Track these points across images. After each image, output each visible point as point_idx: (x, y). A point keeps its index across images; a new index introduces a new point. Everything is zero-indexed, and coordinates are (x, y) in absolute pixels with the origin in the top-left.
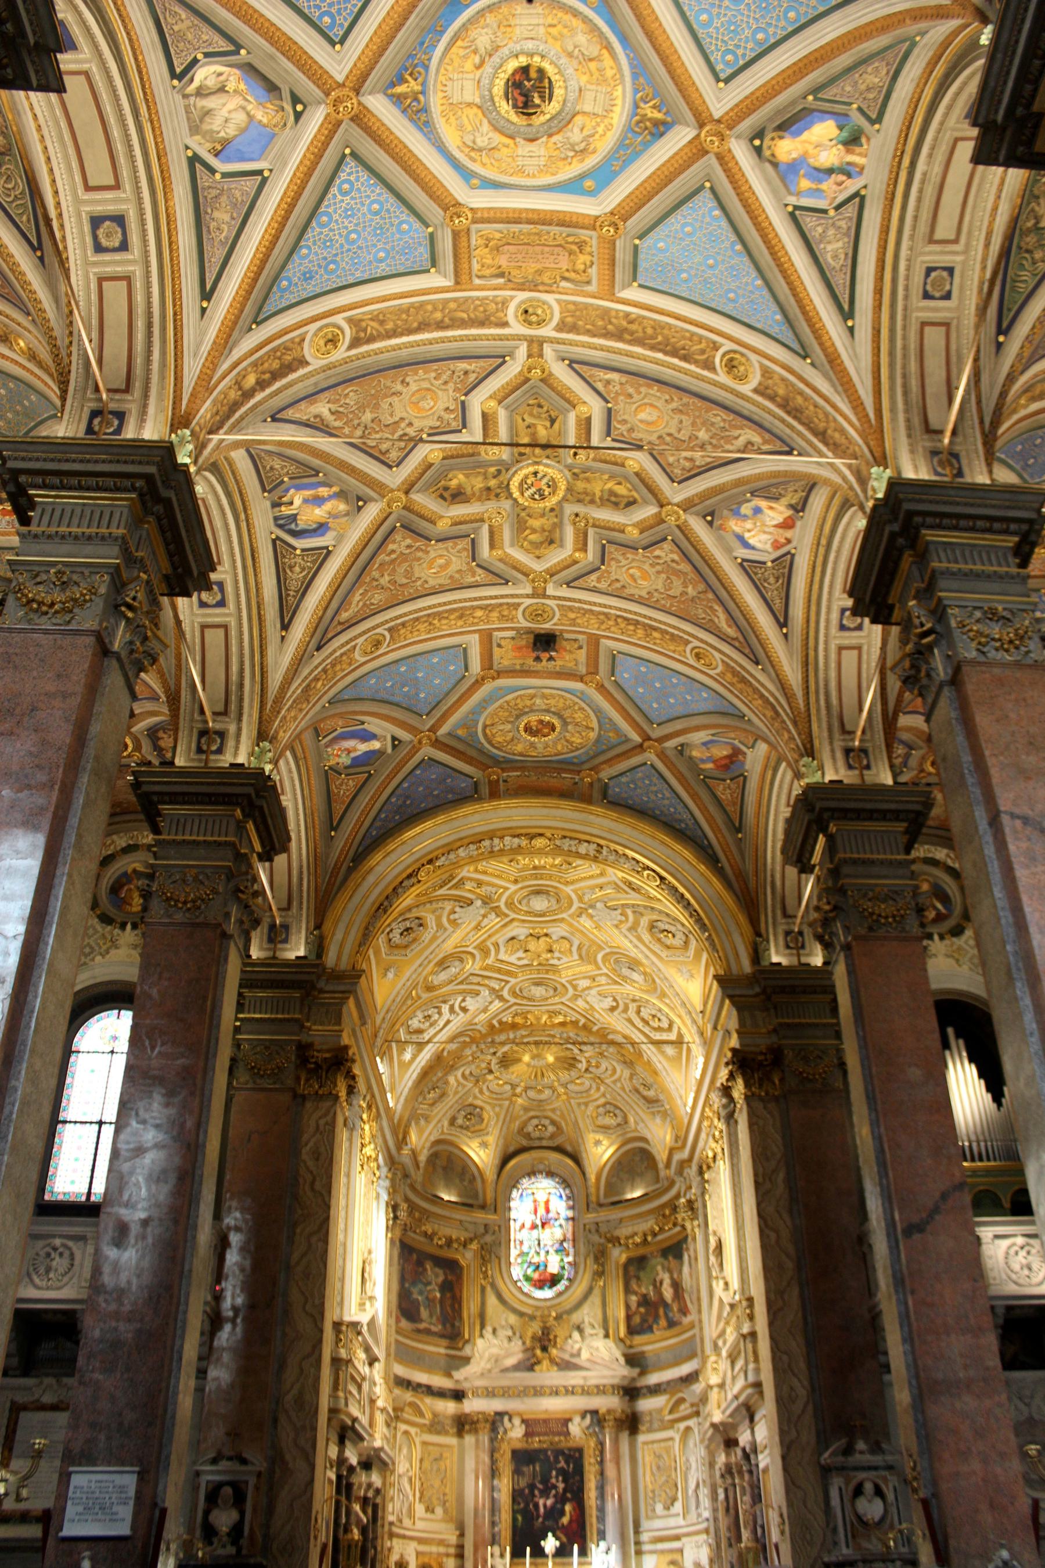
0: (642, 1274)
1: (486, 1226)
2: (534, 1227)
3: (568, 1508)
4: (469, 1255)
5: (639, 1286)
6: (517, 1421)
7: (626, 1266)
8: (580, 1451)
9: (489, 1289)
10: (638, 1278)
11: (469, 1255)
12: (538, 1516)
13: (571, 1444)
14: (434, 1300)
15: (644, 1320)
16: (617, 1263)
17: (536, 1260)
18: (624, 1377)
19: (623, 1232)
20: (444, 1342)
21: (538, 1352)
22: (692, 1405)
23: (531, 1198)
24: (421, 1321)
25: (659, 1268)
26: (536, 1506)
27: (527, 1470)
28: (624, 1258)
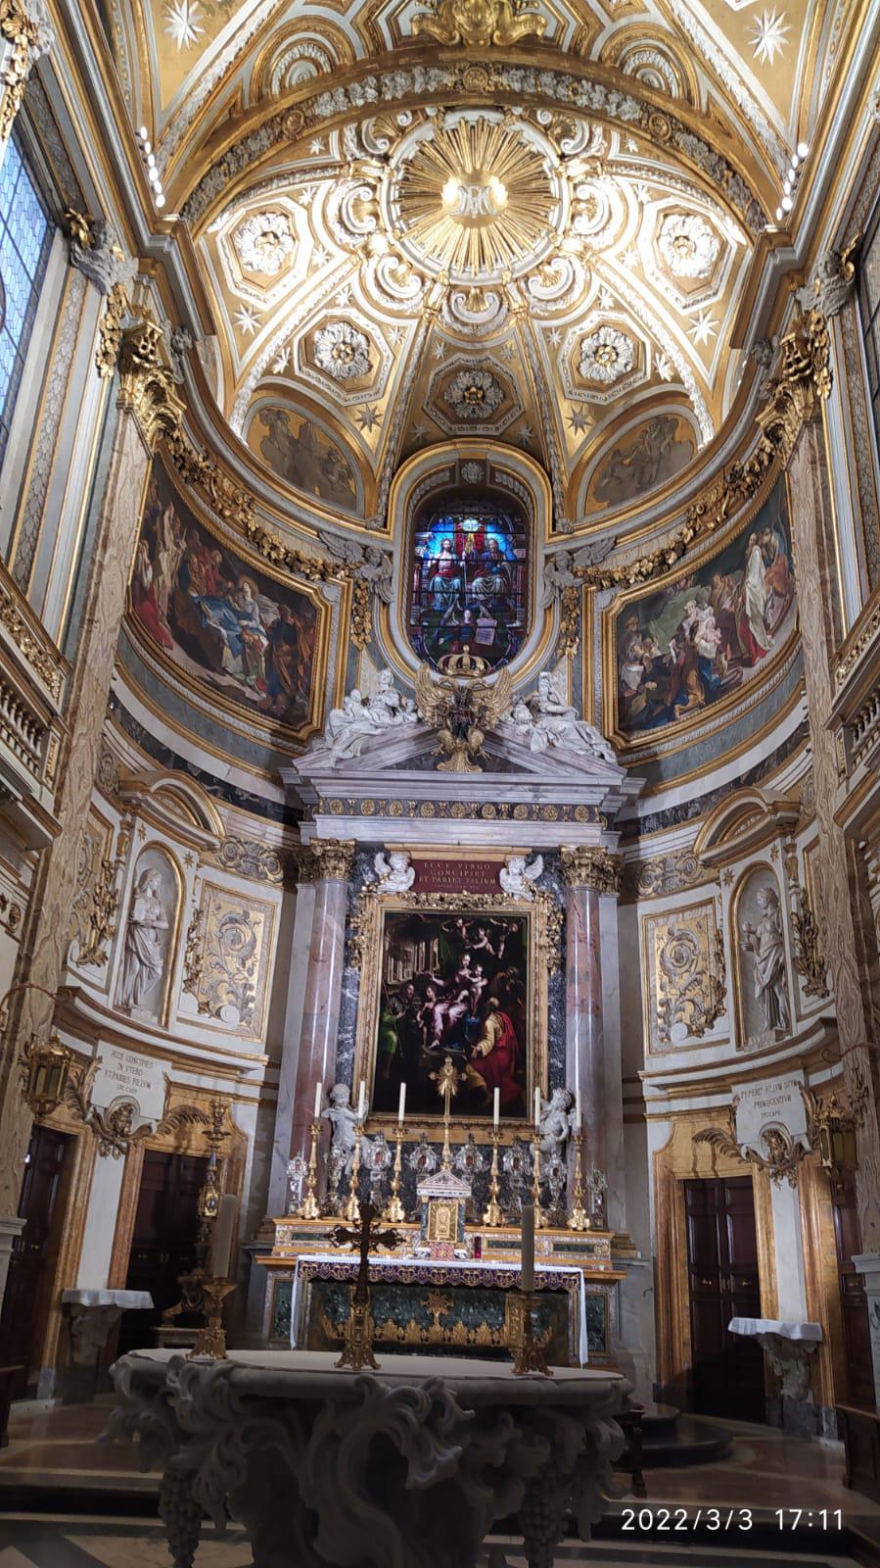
0: (653, 625)
1: (365, 548)
2: (454, 570)
3: (491, 1024)
4: (331, 594)
5: (648, 648)
6: (399, 861)
7: (621, 619)
8: (522, 921)
9: (364, 652)
10: (645, 634)
11: (331, 594)
12: (431, 1036)
13: (505, 908)
14: (257, 644)
15: (654, 700)
16: (605, 615)
17: (455, 622)
18: (614, 790)
19: (615, 564)
20: (273, 724)
21: (447, 735)
22: (775, 807)
23: (452, 527)
24: (224, 672)
25: (691, 604)
26: (429, 1016)
27: (415, 951)
28: (617, 605)
